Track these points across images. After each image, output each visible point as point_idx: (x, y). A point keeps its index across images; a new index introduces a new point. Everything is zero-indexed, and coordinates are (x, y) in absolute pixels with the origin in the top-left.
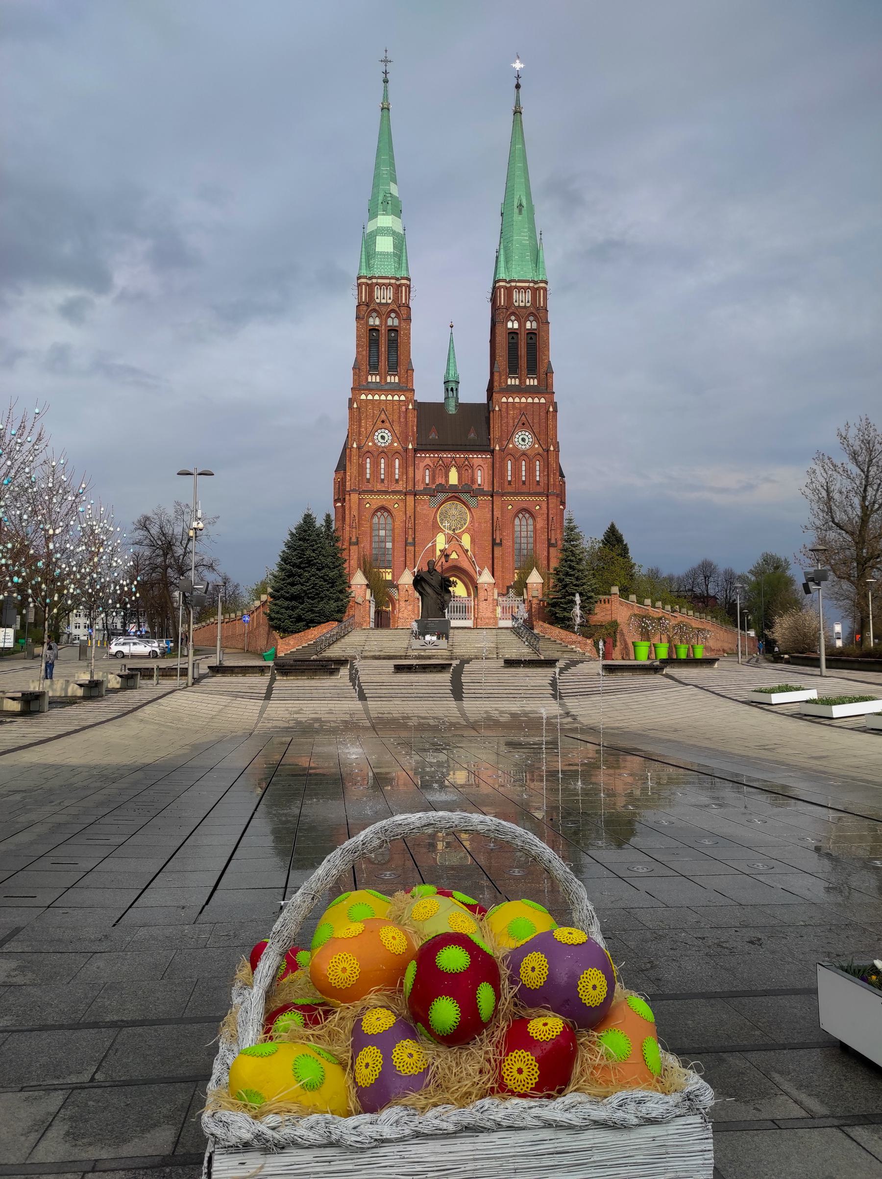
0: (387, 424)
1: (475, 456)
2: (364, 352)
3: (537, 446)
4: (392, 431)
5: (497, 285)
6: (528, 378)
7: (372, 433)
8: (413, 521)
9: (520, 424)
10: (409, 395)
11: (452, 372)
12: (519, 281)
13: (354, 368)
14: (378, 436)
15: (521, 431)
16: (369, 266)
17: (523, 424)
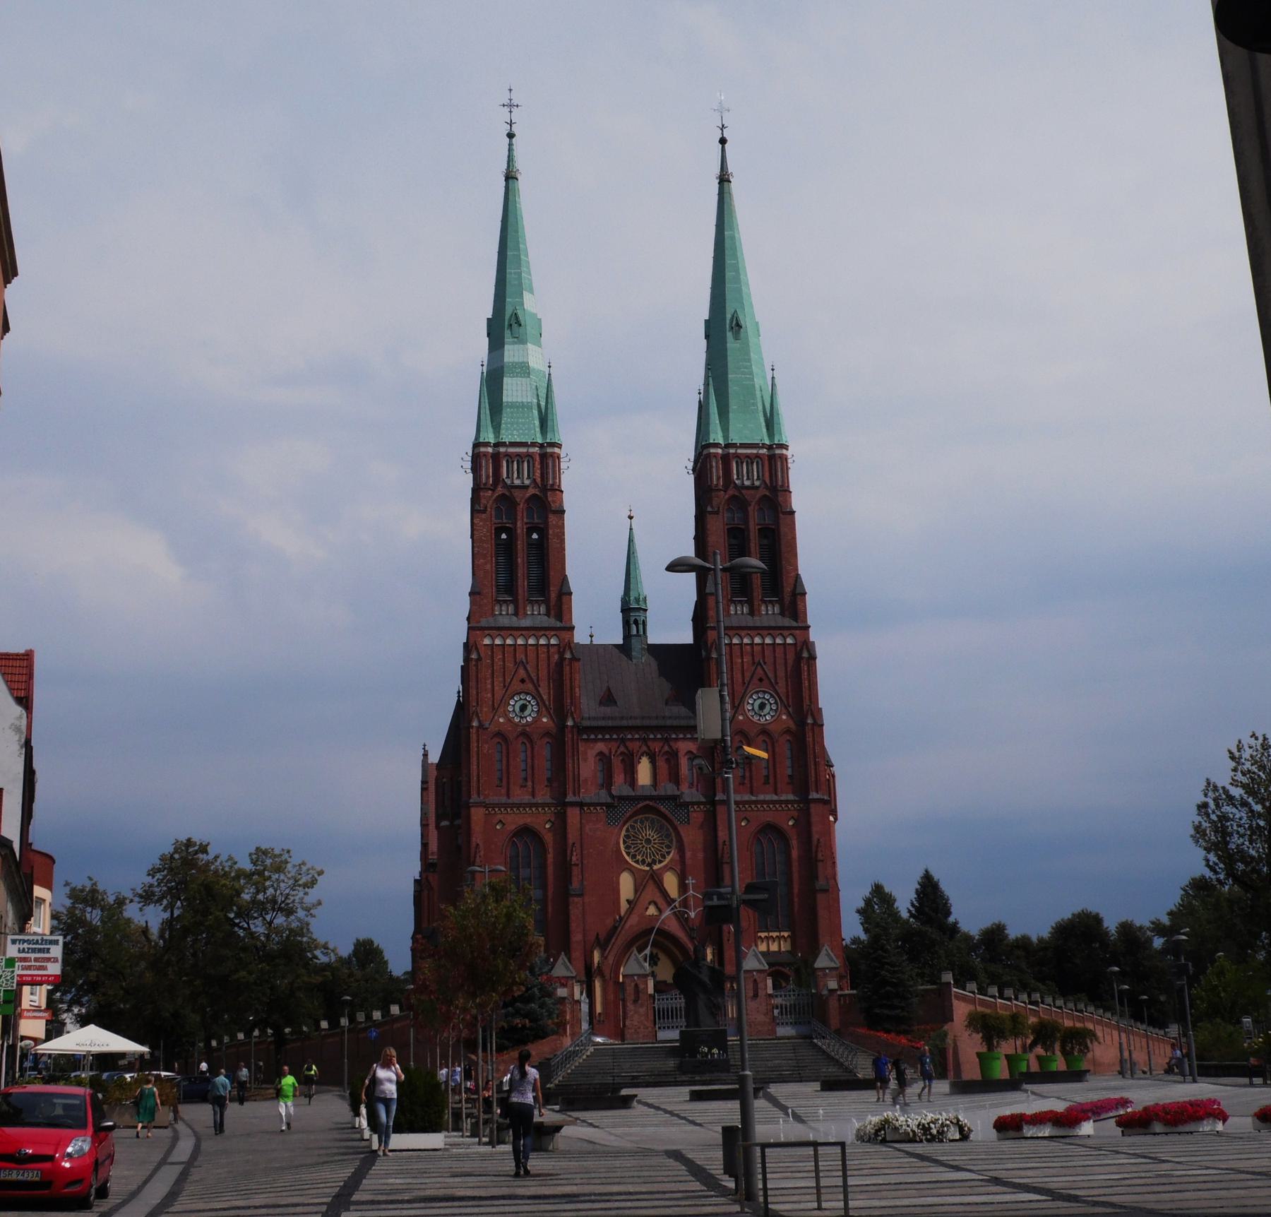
0: (530, 686)
1: (681, 736)
2: (488, 567)
3: (784, 717)
4: (537, 697)
5: (705, 452)
6: (765, 602)
7: (504, 702)
8: (579, 851)
9: (755, 680)
10: (564, 635)
11: (633, 595)
12: (743, 446)
13: (471, 594)
14: (514, 704)
15: (757, 692)
16: (497, 428)
17: (761, 680)
